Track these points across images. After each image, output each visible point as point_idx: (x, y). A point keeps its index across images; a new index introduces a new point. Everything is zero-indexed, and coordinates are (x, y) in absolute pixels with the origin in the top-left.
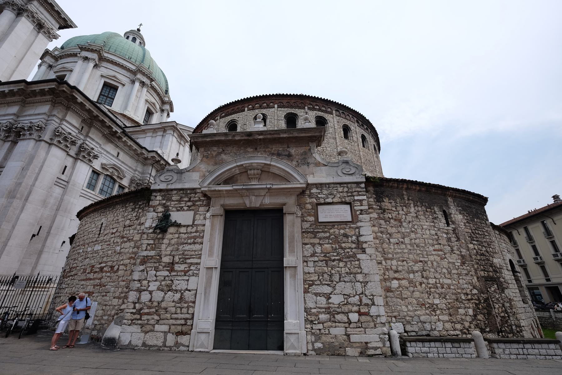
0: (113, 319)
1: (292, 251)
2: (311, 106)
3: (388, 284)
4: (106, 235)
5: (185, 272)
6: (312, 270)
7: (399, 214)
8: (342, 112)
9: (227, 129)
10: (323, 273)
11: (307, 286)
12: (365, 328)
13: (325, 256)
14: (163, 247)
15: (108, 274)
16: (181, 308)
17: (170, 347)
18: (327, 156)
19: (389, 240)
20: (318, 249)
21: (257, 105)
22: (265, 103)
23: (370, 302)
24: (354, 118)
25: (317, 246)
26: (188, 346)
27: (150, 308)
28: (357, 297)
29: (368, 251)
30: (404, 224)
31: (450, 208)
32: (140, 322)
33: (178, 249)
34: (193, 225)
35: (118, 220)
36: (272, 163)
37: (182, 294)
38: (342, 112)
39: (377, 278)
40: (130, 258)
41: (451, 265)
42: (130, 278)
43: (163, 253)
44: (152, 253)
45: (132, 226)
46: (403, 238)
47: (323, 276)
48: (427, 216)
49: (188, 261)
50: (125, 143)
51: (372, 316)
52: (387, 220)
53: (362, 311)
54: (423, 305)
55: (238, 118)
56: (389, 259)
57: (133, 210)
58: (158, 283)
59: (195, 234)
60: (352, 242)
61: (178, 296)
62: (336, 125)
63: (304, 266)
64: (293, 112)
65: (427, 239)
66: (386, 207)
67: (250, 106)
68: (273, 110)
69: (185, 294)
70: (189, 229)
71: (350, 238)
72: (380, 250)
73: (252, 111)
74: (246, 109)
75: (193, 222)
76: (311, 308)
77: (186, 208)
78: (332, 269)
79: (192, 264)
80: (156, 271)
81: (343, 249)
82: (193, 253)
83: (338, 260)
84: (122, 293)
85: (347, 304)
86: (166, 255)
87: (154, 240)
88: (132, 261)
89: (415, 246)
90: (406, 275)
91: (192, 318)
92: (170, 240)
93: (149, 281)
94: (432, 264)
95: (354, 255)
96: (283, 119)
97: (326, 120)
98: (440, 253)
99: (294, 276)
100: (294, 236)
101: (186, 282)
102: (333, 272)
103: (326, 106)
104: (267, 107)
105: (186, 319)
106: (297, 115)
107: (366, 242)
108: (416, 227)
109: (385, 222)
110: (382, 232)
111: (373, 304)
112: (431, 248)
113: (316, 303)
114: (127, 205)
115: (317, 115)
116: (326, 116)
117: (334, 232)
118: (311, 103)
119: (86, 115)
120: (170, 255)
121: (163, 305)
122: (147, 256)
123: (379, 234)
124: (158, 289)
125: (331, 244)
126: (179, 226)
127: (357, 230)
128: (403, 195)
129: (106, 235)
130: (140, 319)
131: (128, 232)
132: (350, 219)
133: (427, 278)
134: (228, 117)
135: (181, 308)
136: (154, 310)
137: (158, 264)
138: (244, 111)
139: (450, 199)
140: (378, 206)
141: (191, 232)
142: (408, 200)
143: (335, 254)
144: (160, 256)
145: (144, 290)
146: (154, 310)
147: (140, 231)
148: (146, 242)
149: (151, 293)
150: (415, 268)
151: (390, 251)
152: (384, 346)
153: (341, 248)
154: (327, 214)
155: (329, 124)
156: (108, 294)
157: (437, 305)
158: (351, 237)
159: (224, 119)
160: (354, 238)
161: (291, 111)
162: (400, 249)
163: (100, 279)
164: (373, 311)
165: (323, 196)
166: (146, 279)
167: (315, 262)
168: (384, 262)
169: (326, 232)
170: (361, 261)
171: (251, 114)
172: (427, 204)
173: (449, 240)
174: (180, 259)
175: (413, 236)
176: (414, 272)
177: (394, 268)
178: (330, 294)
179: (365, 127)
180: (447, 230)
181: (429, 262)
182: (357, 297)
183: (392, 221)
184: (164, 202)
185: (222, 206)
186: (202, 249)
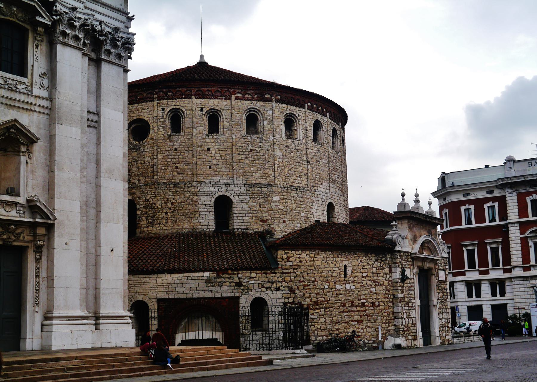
0: (386, 335)
5: (412, 307)
13: (441, 300)
14: (405, 291)
15: (372, 308)
17: (413, 346)
26: (417, 345)
32: (405, 335)
35: (364, 266)
36: (433, 242)
40: (385, 298)
42: (389, 311)
55: (298, 115)
57: (376, 260)
73: (310, 112)
77: (407, 266)
80: (405, 307)
81: (444, 296)
84: (386, 320)
88: (387, 300)
91: (416, 332)
95: (446, 300)
105: (415, 333)
106: (337, 133)
114: (369, 255)
130: (404, 334)
131: (377, 278)
134: (286, 106)
144: (404, 297)
147: (386, 279)
156: (377, 321)
159: (280, 105)
163: (366, 311)
184: (400, 260)
185: (418, 267)
186: (415, 294)
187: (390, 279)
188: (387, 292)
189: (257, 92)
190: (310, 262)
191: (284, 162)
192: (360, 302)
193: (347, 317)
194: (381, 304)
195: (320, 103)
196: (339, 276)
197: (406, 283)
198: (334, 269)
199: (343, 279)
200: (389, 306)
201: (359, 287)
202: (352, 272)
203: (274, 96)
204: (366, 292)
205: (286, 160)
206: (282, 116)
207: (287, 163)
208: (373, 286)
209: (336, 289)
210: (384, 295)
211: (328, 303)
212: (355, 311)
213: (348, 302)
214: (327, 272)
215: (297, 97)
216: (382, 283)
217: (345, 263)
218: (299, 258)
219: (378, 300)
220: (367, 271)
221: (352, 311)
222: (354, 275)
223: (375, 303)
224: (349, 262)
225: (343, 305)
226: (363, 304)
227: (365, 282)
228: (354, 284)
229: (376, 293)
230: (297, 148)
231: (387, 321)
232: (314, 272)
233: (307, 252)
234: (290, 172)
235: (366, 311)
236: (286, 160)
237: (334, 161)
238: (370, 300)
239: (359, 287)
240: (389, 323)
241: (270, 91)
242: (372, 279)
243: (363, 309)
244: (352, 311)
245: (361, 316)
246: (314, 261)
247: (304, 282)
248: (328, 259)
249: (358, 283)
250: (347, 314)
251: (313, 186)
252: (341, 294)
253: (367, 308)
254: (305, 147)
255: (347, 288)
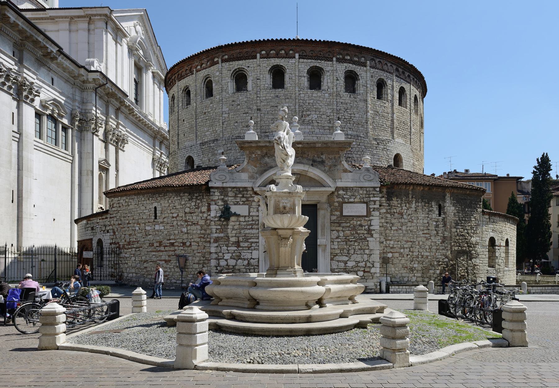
1: (323, 235)
2: (341, 56)
3: (385, 255)
4: (165, 218)
5: (249, 248)
6: (336, 247)
7: (402, 209)
8: (380, 62)
9: (233, 79)
10: (344, 249)
11: (333, 257)
12: (366, 279)
14: (229, 231)
15: (182, 248)
16: (250, 269)
18: (355, 125)
19: (391, 227)
20: (341, 234)
21: (272, 52)
22: (282, 50)
23: (371, 266)
24: (392, 67)
25: (341, 232)
27: (227, 269)
28: (364, 263)
29: (375, 235)
30: (405, 216)
31: (445, 202)
33: (240, 233)
34: (249, 216)
37: (249, 261)
38: (380, 62)
39: (378, 252)
41: (433, 244)
42: (204, 251)
43: (230, 235)
44: (222, 235)
45: (193, 213)
46: (402, 227)
47: (343, 251)
48: (424, 210)
49: (250, 241)
50: (59, 65)
51: (371, 273)
52: (392, 214)
53: (366, 270)
54: (407, 267)
55: (248, 67)
56: (388, 240)
58: (230, 255)
59: (251, 222)
60: (365, 230)
61: (246, 262)
62: (368, 82)
63: (331, 245)
64: (318, 65)
65: (420, 226)
66: (394, 205)
67: (263, 52)
68: (292, 61)
69: (251, 261)
70: (247, 219)
71: (364, 228)
72: (384, 234)
73: (266, 59)
74: (258, 55)
75: (249, 214)
76: (334, 269)
78: (350, 247)
79: (252, 242)
80: (227, 247)
82: (252, 235)
83: (354, 241)
85: (357, 266)
86: (232, 237)
87: (221, 226)
89: (409, 231)
90: (398, 250)
92: (233, 226)
93: (223, 254)
94: (419, 243)
95: (365, 238)
96: (305, 75)
97: (358, 75)
98: (427, 236)
99: (324, 250)
100: (324, 225)
101: (250, 254)
102: (350, 248)
103: (360, 56)
104: (285, 56)
106: (323, 70)
107: (374, 230)
108: (413, 218)
109: (391, 215)
110: (387, 223)
111: (373, 267)
112: (421, 233)
113: (338, 266)
115: (347, 69)
116: (358, 70)
117: (353, 223)
118: (341, 52)
119: (18, 37)
120: (235, 236)
121: (237, 267)
122: (218, 237)
123: (385, 224)
124: (231, 258)
125: (350, 231)
126: (239, 216)
127: (369, 222)
128: (409, 194)
129: (165, 218)
131: (191, 218)
132: (365, 214)
133: (413, 252)
134: (234, 62)
135: (250, 269)
136: (231, 270)
137: (227, 242)
138: (255, 57)
139: (448, 195)
140: (387, 203)
141: (248, 221)
142: (412, 197)
143: (353, 237)
144: (228, 237)
145: (221, 259)
146: (231, 270)
147: (203, 218)
148: (215, 227)
149: (226, 260)
150: (405, 246)
151: (390, 235)
152: (376, 288)
153: (357, 233)
154: (349, 210)
155: (361, 81)
157: (415, 268)
158: (365, 226)
159: (227, 64)
160: (367, 227)
161: (315, 64)
162: (398, 234)
164: (373, 270)
165: (347, 197)
166: (221, 252)
167: (338, 242)
168: (385, 243)
169: (348, 223)
170: (369, 242)
171: (265, 65)
172: (426, 201)
173: (437, 226)
174: (243, 239)
175: (409, 224)
176: (404, 248)
177: (391, 246)
178: (348, 261)
179: (407, 75)
180: (438, 219)
181: (417, 243)
182: (364, 263)
183: (396, 214)
187: (209, 218)
188: (203, 232)
189: (208, 58)
190: (126, 206)
191: (230, 116)
192: (168, 242)
193: (154, 256)
194: (192, 244)
195: (281, 48)
196: (149, 218)
197: (233, 221)
198: (145, 211)
199: (152, 220)
200: (205, 246)
201: (169, 227)
202: (161, 213)
203: (220, 57)
204: (176, 232)
205: (232, 114)
206: (229, 73)
207: (233, 116)
208: (185, 226)
209: (145, 230)
210: (199, 234)
211: (138, 243)
212: (163, 251)
213: (157, 242)
214: (138, 215)
215: (245, 50)
216: (196, 222)
217: (155, 204)
218: (119, 203)
219: (190, 241)
220: (177, 211)
221: (160, 251)
222: (163, 216)
223: (186, 243)
224: (159, 204)
225: (151, 245)
226: (172, 244)
227: (175, 223)
228: (163, 225)
229: (187, 233)
230: (245, 99)
231: (202, 262)
232: (128, 215)
233: (124, 198)
234: (236, 124)
235: (175, 250)
236: (232, 114)
237: (312, 101)
238: (181, 241)
239: (169, 227)
240: (204, 263)
241: (216, 54)
242: (184, 219)
243: (172, 249)
244: (160, 251)
245: (169, 256)
246: (129, 205)
247: (121, 224)
248: (139, 203)
249: (168, 223)
250: (154, 253)
251: (266, 132)
252: (150, 235)
253: (176, 248)
254: (255, 96)
255: (156, 229)
